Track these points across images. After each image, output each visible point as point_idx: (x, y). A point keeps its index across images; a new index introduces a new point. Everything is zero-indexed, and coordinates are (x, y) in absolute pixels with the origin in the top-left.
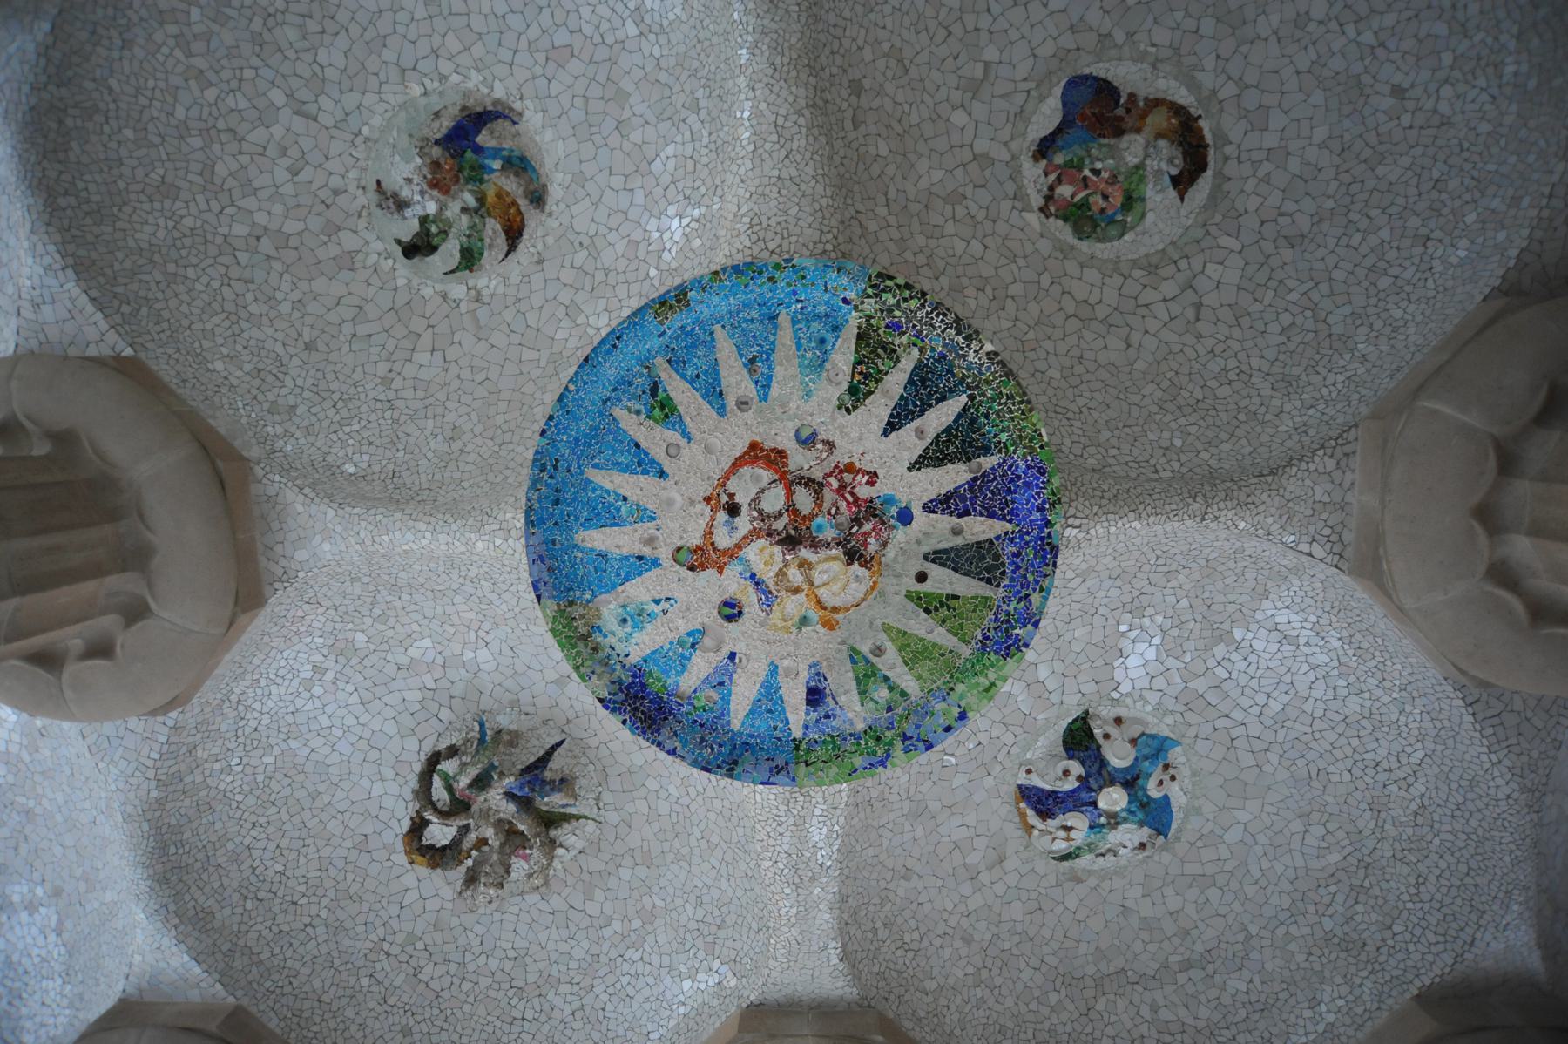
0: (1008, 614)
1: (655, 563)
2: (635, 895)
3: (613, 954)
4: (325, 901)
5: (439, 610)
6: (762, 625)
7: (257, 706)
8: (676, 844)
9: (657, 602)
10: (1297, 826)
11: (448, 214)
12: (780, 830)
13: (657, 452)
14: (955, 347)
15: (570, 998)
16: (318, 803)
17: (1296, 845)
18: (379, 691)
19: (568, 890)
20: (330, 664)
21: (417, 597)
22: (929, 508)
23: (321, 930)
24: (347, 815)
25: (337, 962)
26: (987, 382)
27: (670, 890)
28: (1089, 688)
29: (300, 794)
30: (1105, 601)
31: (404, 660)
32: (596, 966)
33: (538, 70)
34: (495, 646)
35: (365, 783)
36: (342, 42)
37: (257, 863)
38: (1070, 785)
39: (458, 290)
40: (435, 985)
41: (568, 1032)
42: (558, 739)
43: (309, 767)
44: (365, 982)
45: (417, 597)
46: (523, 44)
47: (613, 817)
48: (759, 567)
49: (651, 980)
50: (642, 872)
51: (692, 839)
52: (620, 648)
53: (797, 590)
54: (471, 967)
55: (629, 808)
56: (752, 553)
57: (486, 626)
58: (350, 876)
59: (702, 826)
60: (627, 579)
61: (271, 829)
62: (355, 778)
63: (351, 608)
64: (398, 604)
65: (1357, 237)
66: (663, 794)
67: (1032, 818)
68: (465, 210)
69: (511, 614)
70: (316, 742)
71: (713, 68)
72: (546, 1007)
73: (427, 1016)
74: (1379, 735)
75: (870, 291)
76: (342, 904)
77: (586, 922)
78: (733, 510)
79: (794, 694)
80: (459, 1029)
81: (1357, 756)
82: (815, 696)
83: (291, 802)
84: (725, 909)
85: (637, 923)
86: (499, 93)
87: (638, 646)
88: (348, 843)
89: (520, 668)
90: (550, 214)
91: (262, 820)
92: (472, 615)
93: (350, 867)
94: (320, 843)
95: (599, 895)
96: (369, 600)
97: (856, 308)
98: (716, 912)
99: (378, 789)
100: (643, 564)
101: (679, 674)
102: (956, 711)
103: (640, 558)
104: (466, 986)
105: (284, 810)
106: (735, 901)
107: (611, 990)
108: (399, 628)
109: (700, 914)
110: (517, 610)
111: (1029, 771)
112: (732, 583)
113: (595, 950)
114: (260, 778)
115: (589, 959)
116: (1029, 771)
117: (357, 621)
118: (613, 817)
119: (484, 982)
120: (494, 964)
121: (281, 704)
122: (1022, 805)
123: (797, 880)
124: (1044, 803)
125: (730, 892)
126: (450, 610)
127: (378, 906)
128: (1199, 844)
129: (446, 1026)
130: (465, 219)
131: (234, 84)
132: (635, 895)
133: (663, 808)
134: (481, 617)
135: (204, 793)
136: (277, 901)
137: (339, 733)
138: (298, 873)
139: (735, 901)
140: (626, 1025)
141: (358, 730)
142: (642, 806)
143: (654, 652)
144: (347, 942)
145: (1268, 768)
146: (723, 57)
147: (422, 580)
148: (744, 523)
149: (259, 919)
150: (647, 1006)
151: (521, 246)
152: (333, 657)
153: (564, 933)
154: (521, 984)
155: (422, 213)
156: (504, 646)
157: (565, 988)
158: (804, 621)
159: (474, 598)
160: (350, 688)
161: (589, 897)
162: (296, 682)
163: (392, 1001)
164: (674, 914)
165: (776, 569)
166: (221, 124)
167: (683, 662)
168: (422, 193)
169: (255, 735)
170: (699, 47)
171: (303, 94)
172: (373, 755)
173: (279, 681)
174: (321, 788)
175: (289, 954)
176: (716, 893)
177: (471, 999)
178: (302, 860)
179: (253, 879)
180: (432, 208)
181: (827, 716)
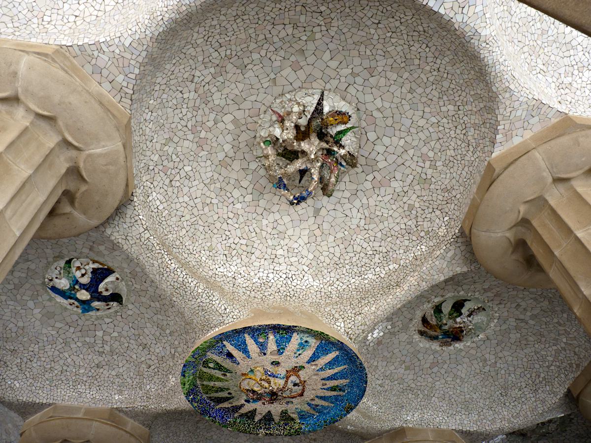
0: (198, 395)
1: (308, 362)
2: (215, 145)
3: (200, 112)
4: (376, 37)
5: (386, 223)
6: (263, 366)
7: (459, 143)
8: (218, 185)
9: (299, 355)
10: (20, 324)
11: (451, 321)
12: (200, 308)
13: (327, 382)
14: (268, 429)
15: (202, 78)
16: (407, 86)
17: (12, 320)
18: (400, 161)
19: (247, 115)
20: (429, 172)
21: (397, 228)
22: (242, 405)
23: (369, 23)
24: (388, 84)
25: (347, 10)
26: (254, 428)
27: (203, 164)
28: (130, 312)
29: (419, 91)
30: (157, 346)
31: (394, 184)
32: (203, 100)
33: (439, 358)
34: (355, 211)
35: (387, 105)
36: (513, 341)
37: (427, 49)
38: (101, 287)
39: (437, 300)
40: (281, 27)
41: (188, 69)
42: (303, 181)
43: (421, 107)
44: (323, 8)
45: (397, 228)
46: (448, 362)
47: (253, 166)
48: (277, 380)
49: (173, 126)
50: (221, 156)
51: (213, 195)
52: (302, 335)
53: (261, 380)
54: (266, 46)
55: (250, 177)
56: (282, 382)
57: (363, 222)
58: (368, 53)
59: (215, 206)
60: (314, 354)
61: (428, 68)
62: (394, 106)
63: (426, 211)
64: (406, 220)
65: (185, 433)
66: (241, 199)
67: (96, 266)
68: (446, 324)
69: (354, 238)
70: (422, 122)
71: (381, 397)
72: (210, 65)
73: (271, 14)
74: (42, 368)
75: (299, 430)
76: (365, 39)
77: (225, 111)
78: (295, 385)
79: (235, 352)
80: (248, 21)
81: (37, 356)
82: (230, 355)
83: (422, 85)
84: (176, 191)
85: (203, 134)
86: (452, 348)
87: (296, 339)
88: (380, 69)
89: (338, 207)
90: (415, 331)
91: (435, 73)
92: (372, 226)
93: (372, 58)
94: (395, 65)
95: (231, 127)
96: (419, 219)
97: (300, 423)
98: (178, 184)
99: (379, 103)
100: (313, 359)
101: (277, 340)
102: (186, 375)
103: (314, 361)
104: (261, 37)
105: (425, 80)
106: (176, 200)
107: (186, 101)
108: (401, 203)
109: (183, 174)
110: (352, 242)
111: (117, 279)
112: (281, 371)
113: (210, 105)
114: (445, 98)
115: (209, 99)
116: (117, 279)
117: (422, 203)
118: (253, 166)
119: (253, 46)
120: (255, 56)
121: (447, 144)
122: (106, 267)
123: (177, 291)
124: (100, 274)
125: (181, 200)
126: (381, 226)
127: (343, 44)
128: (36, 293)
129: (256, 17)
130: (445, 322)
131: (548, 324)
132: (215, 145)
133: (236, 193)
134: (366, 227)
135: (472, 93)
136: (404, 32)
137: (413, 130)
138: (399, 48)
139: (176, 200)
140: (164, 101)
141: (403, 135)
142: (245, 183)
143: (290, 341)
144: (349, 21)
145: (50, 328)
146: (379, 403)
147: (398, 242)
148: (290, 385)
149: (410, 22)
150: (164, 118)
151: (421, 319)
152: (429, 177)
153: (232, 96)
154: (231, 61)
155: (462, 316)
156: (349, 214)
157: (210, 77)
158: (252, 371)
159: (372, 239)
160: (415, 158)
161: (235, 121)
162: (443, 159)
163: (298, 8)
164: (192, 158)
165: (272, 383)
166: (550, 313)
167: (278, 343)
168: (464, 322)
169: (456, 124)
170: (388, 397)
171: (522, 324)
172: (389, 122)
173: (452, 159)
174: (409, 96)
175: (381, 8)
176: (186, 190)
177: (253, 35)
178: (401, 54)
179: (425, 41)
180: (458, 320)
181: (221, 352)
